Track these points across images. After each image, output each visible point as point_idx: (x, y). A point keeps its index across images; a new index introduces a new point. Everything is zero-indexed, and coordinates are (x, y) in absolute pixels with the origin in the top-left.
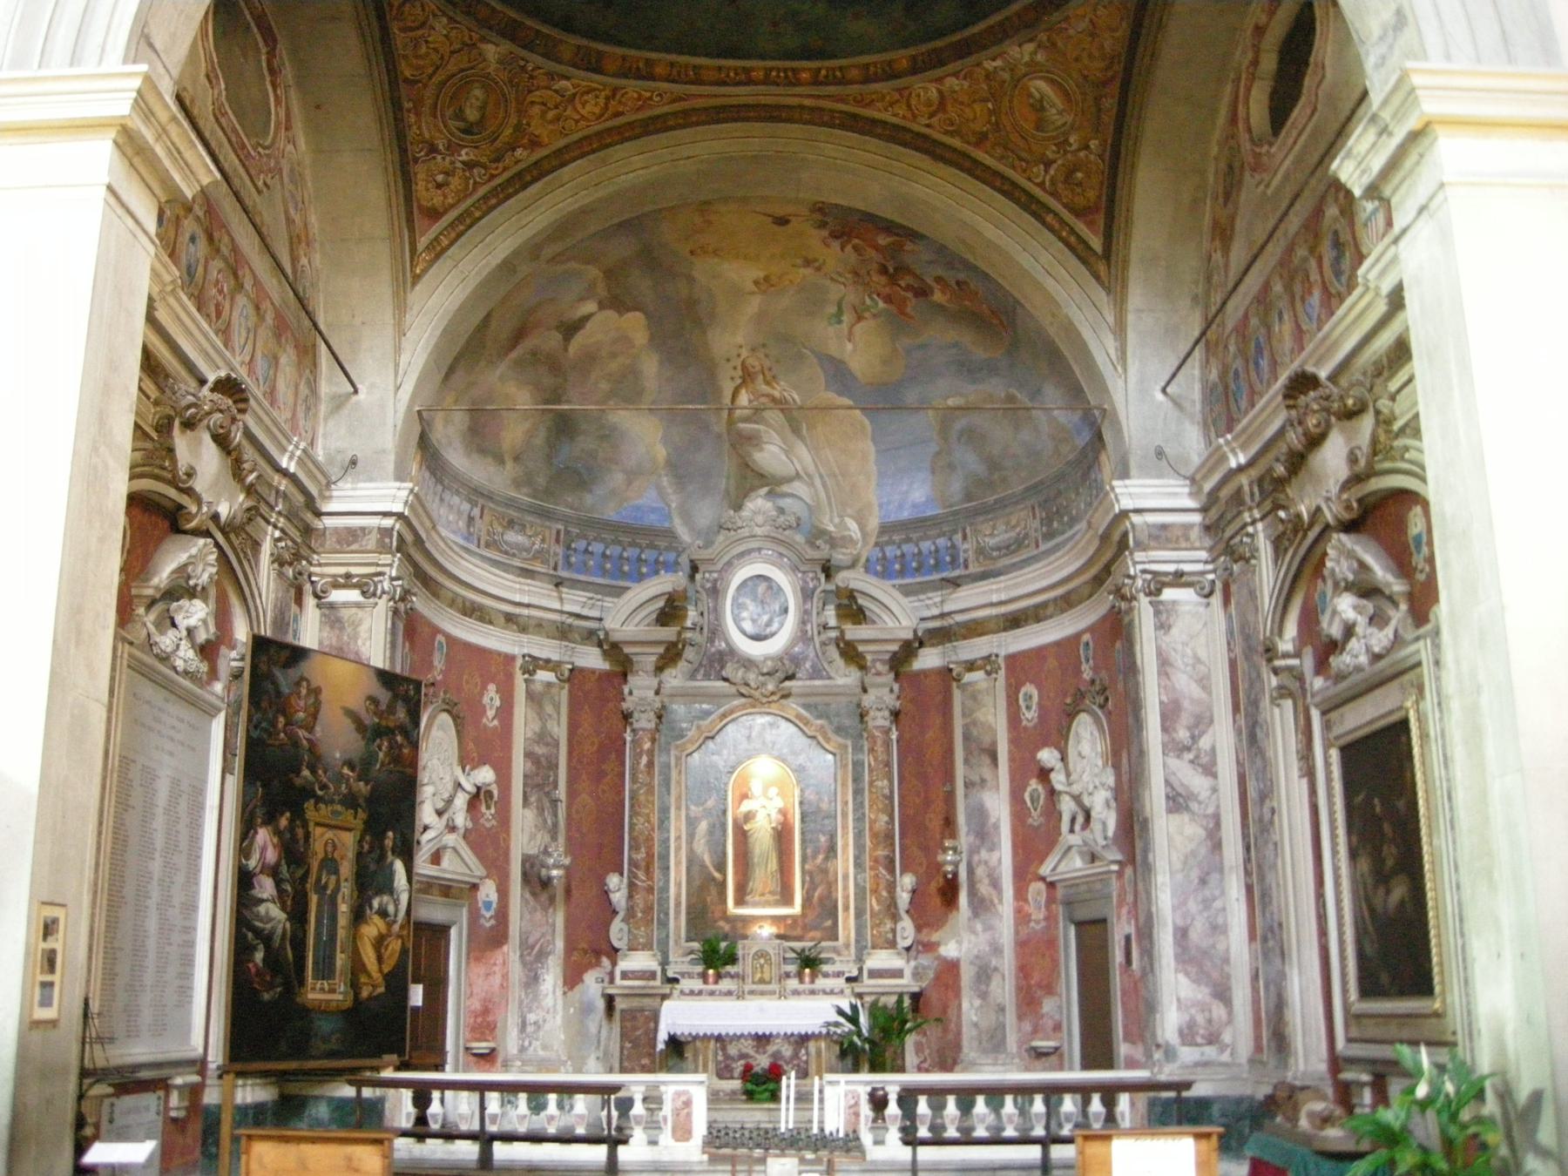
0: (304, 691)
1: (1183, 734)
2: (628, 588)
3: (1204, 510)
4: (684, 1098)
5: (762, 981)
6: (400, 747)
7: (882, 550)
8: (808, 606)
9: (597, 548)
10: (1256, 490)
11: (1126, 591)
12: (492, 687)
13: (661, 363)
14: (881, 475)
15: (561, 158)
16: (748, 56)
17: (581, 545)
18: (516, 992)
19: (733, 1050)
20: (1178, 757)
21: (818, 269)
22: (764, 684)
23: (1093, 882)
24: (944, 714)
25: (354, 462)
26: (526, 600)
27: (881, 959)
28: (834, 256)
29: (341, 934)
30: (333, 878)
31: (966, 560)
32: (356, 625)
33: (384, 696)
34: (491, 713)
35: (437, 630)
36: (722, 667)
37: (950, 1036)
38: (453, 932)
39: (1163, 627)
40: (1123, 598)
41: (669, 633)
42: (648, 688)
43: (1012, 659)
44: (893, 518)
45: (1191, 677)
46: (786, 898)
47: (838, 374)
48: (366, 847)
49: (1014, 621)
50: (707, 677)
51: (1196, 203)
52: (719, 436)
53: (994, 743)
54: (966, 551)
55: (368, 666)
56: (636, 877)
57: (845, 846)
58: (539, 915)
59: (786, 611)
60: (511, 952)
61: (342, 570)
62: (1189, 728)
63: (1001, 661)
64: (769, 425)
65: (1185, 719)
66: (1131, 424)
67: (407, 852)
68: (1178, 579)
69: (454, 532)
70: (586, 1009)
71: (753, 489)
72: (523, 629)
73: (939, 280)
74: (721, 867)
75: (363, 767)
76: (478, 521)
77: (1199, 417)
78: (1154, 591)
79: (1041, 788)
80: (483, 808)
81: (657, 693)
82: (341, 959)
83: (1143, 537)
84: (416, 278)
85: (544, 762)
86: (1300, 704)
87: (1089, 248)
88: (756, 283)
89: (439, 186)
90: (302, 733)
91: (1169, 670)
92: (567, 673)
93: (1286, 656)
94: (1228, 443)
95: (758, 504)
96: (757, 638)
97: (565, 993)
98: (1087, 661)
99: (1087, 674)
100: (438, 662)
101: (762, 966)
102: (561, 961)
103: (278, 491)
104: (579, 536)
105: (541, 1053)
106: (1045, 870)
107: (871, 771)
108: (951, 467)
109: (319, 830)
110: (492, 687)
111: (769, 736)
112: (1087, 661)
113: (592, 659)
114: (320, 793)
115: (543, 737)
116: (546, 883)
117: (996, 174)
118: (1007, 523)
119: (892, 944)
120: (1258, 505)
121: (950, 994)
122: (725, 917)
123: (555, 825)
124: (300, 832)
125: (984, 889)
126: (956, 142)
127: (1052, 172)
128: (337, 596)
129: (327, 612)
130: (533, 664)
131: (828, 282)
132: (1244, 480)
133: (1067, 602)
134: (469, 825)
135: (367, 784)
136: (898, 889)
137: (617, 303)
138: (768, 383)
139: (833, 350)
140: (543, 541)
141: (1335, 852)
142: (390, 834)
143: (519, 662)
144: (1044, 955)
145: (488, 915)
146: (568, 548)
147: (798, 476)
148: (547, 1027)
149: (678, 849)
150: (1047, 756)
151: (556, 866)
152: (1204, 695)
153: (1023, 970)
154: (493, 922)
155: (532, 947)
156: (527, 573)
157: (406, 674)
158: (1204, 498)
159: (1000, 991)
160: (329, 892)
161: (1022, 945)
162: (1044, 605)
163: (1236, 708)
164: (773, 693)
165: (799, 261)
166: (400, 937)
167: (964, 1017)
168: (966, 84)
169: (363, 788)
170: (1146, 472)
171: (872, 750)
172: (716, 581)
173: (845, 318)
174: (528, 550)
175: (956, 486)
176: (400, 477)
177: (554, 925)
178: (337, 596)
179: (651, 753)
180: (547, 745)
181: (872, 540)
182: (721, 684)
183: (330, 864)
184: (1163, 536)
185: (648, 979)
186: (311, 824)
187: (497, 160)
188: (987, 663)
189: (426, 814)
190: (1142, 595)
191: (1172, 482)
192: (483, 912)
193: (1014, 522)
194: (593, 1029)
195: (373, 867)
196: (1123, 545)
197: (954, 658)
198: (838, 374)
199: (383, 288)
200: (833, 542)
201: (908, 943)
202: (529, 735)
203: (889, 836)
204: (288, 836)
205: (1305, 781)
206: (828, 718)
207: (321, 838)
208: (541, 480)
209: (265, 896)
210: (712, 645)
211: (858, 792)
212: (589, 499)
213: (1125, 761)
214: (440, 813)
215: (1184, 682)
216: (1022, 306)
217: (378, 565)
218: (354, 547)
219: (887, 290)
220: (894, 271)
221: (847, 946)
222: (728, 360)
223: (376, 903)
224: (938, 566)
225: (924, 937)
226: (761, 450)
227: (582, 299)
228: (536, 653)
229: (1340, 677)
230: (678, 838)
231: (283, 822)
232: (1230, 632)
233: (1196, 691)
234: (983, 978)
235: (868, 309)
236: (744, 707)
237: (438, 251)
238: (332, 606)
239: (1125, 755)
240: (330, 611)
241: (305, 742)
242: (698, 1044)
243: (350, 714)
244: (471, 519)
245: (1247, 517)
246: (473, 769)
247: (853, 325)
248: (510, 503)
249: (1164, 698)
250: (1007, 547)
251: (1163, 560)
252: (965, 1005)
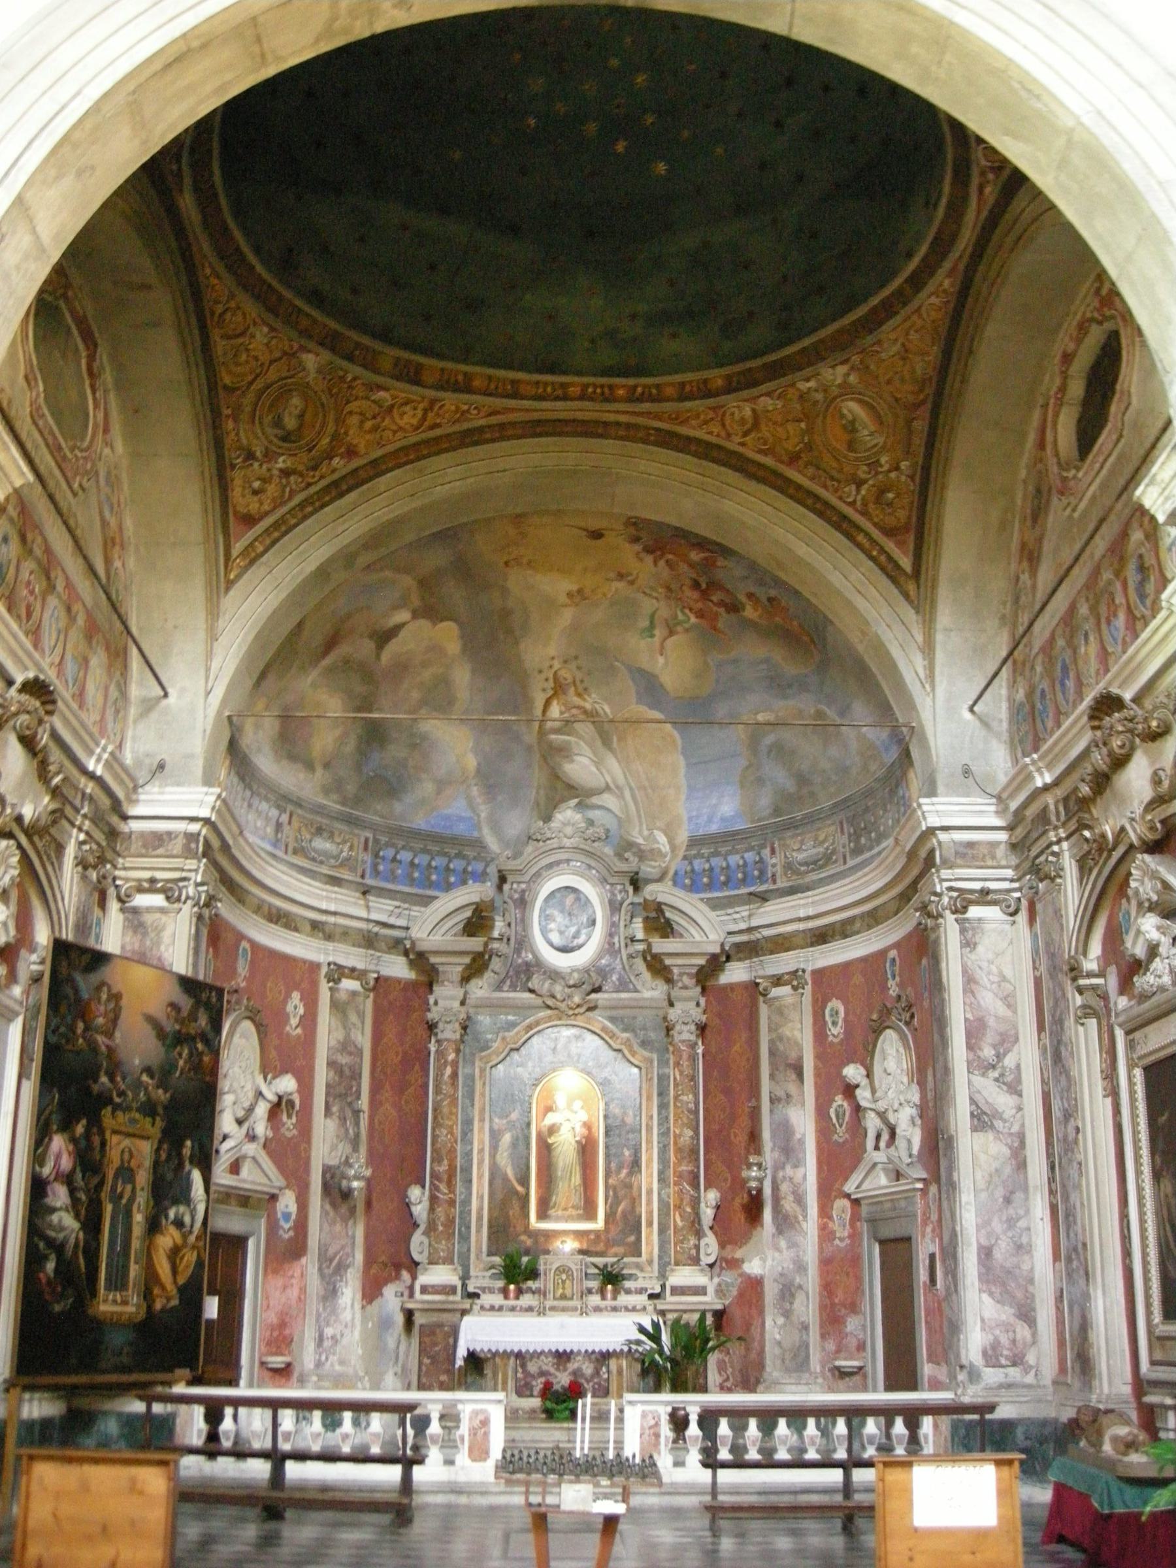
0: (104, 997)
1: (988, 1053)
2: (436, 898)
3: (1010, 828)
4: (481, 1417)
5: (563, 1297)
6: (202, 1054)
7: (691, 863)
8: (616, 919)
9: (405, 856)
10: (1061, 809)
11: (932, 908)
12: (296, 996)
13: (473, 671)
14: (691, 789)
15: (376, 469)
16: (564, 373)
17: (389, 853)
18: (313, 1305)
19: (532, 1367)
20: (983, 1075)
21: (632, 583)
22: (570, 996)
24: (750, 1029)
25: (161, 766)
26: (332, 908)
27: (683, 1276)
28: (647, 569)
29: (135, 1244)
30: (129, 1187)
31: (774, 875)
32: (159, 930)
33: (186, 1003)
34: (294, 1021)
35: (241, 937)
36: (529, 979)
37: (753, 1355)
38: (251, 1244)
39: (968, 944)
40: (930, 915)
41: (475, 944)
42: (452, 998)
43: (819, 975)
44: (701, 832)
45: (996, 995)
46: (589, 1212)
47: (650, 689)
48: (164, 1156)
49: (821, 937)
50: (513, 988)
51: (1004, 525)
52: (529, 748)
53: (800, 1058)
54: (774, 866)
55: (171, 972)
56: (437, 1189)
57: (650, 1160)
58: (338, 1227)
59: (593, 923)
60: (309, 1264)
61: (147, 875)
62: (994, 1047)
64: (580, 737)
65: (990, 1037)
66: (939, 743)
67: (205, 1161)
68: (984, 897)
69: (263, 839)
70: (385, 1324)
71: (563, 800)
72: (329, 937)
73: (750, 596)
74: (524, 1181)
75: (163, 1074)
76: (286, 828)
77: (1005, 736)
78: (960, 910)
79: (845, 1104)
80: (284, 1117)
81: (463, 1003)
82: (134, 1270)
83: (950, 854)
84: (230, 584)
85: (347, 1072)
86: (1104, 1023)
87: (897, 566)
88: (570, 595)
89: (255, 492)
90: (100, 1039)
91: (973, 986)
92: (372, 983)
93: (1090, 975)
94: (1034, 762)
95: (567, 815)
96: (564, 950)
97: (363, 1307)
98: (894, 977)
99: (893, 991)
100: (242, 968)
101: (564, 1282)
102: (360, 1275)
103: (84, 794)
104: (387, 845)
105: (337, 1368)
106: (850, 1187)
107: (676, 1085)
108: (760, 781)
109: (115, 1139)
110: (296, 996)
111: (574, 1048)
112: (894, 977)
113: (398, 968)
114: (117, 1100)
115: (346, 1046)
116: (346, 1195)
117: (810, 493)
118: (816, 839)
119: (696, 1261)
120: (1064, 824)
121: (754, 1312)
122: (527, 1231)
123: (357, 1135)
124: (96, 1140)
125: (788, 1205)
126: (768, 461)
127: (863, 492)
128: (142, 900)
129: (130, 916)
130: (338, 973)
131: (640, 596)
132: (1050, 799)
133: (873, 919)
134: (270, 1134)
135: (166, 1091)
136: (703, 1205)
137: (430, 612)
138: (579, 695)
139: (644, 662)
140: (351, 848)
141: (1138, 1173)
142: (189, 1143)
143: (324, 970)
145: (287, 1226)
146: (376, 856)
147: (607, 788)
148: (345, 1341)
149: (481, 1162)
150: (853, 1072)
151: (357, 1178)
152: (1009, 1013)
153: (827, 1288)
154: (291, 1233)
155: (331, 1261)
156: (335, 881)
157: (209, 981)
158: (1010, 817)
160: (124, 1201)
161: (826, 1262)
162: (851, 921)
163: (1041, 1028)
164: (578, 1006)
165: (612, 575)
166: (194, 1247)
167: (767, 1336)
168: (780, 404)
169: (161, 1095)
170: (953, 790)
171: (677, 1064)
172: (523, 891)
173: (657, 632)
174: (336, 857)
175: (765, 801)
176: (208, 781)
177: (354, 1237)
178: (142, 900)
179: (455, 1064)
180: (350, 1054)
181: (681, 853)
182: (527, 995)
183: (126, 1173)
184: (969, 854)
185: (447, 1294)
186: (108, 1134)
187: (315, 468)
188: (794, 978)
189: (226, 1122)
190: (948, 912)
191: (979, 800)
192: (282, 1223)
193: (821, 838)
194: (391, 1342)
195: (169, 1176)
196: (929, 862)
197: (761, 973)
198: (650, 689)
199: (197, 592)
200: (642, 855)
201: (711, 1260)
202: (333, 1043)
203: (694, 1151)
204: (83, 1143)
205: (1109, 1100)
206: (633, 1031)
207: (117, 1146)
208: (351, 788)
209: (58, 1204)
210: (519, 956)
211: (663, 1106)
212: (398, 807)
213: (930, 1078)
214: (240, 1122)
215: (989, 1001)
216: (831, 622)
217: (183, 870)
218: (160, 851)
219: (700, 605)
220: (705, 587)
221: (650, 1262)
222: (540, 672)
223: (172, 1213)
224: (744, 882)
225: (729, 1252)
226: (572, 761)
227: (396, 607)
228: (342, 961)
229: (1144, 997)
230: (481, 1151)
231: (80, 1129)
232: (1035, 951)
233: (1002, 1010)
235: (680, 623)
236: (550, 1018)
237: (252, 558)
238: (135, 911)
239: (930, 1073)
240: (134, 916)
241: (103, 1048)
242: (497, 1360)
243: (151, 1020)
244: (279, 826)
245: (1052, 836)
246: (274, 1078)
247: (665, 639)
248: (319, 810)
249: (969, 1016)
250: (815, 863)
251: (970, 878)
252: (769, 1323)
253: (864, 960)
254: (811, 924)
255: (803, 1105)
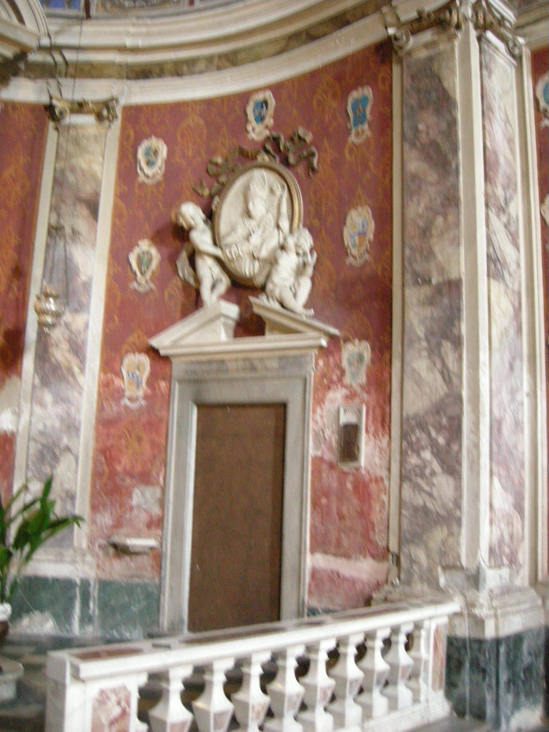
23: (268, 358)
24: (31, 154)
53: (97, 194)
63: (119, 112)
79: (154, 251)
144: (139, 440)
159: (70, 475)
162: (192, 62)
234: (48, 457)
253: (208, 103)
254: (131, 59)
255: (94, 244)
